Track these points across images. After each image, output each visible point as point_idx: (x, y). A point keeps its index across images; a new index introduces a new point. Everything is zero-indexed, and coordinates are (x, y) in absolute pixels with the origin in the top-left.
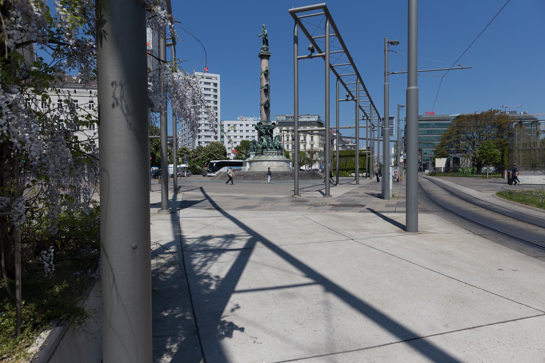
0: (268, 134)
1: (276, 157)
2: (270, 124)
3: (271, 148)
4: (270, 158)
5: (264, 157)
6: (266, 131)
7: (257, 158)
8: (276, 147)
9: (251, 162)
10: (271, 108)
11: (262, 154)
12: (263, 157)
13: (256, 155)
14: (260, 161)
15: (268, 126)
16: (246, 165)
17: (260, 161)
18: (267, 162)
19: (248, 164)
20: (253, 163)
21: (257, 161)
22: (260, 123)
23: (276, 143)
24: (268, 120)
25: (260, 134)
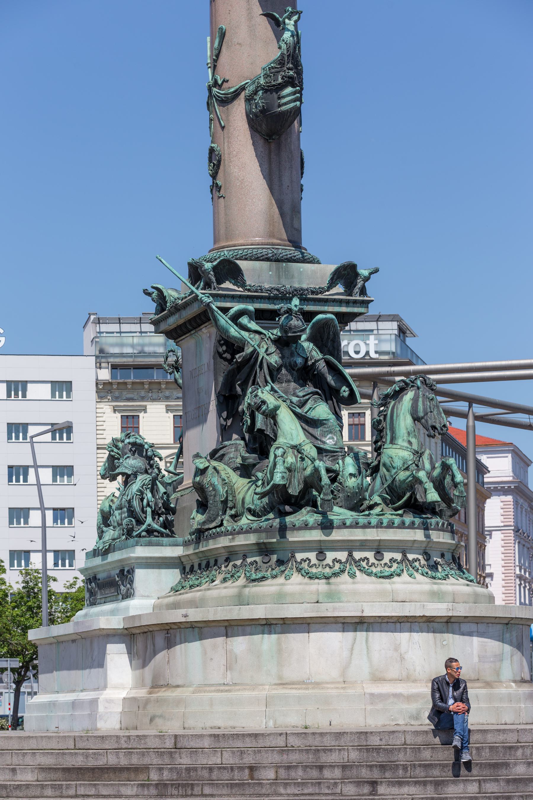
0: (306, 374)
1: (413, 591)
2: (315, 275)
3: (357, 503)
4: (362, 593)
5: (295, 583)
6: (286, 343)
7: (217, 597)
8: (405, 500)
9: (148, 640)
10: (311, 136)
11: (274, 555)
12: (291, 592)
13: (193, 569)
14: (268, 626)
15: (302, 295)
16: (99, 662)
17: (268, 626)
18: (334, 640)
19: (117, 657)
20: (190, 655)
21: (230, 628)
22: (228, 270)
23: (398, 453)
24: (292, 247)
25: (238, 371)
